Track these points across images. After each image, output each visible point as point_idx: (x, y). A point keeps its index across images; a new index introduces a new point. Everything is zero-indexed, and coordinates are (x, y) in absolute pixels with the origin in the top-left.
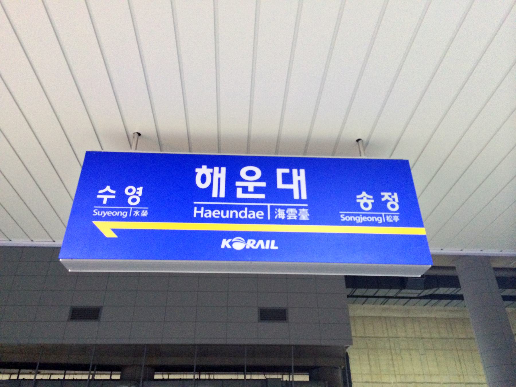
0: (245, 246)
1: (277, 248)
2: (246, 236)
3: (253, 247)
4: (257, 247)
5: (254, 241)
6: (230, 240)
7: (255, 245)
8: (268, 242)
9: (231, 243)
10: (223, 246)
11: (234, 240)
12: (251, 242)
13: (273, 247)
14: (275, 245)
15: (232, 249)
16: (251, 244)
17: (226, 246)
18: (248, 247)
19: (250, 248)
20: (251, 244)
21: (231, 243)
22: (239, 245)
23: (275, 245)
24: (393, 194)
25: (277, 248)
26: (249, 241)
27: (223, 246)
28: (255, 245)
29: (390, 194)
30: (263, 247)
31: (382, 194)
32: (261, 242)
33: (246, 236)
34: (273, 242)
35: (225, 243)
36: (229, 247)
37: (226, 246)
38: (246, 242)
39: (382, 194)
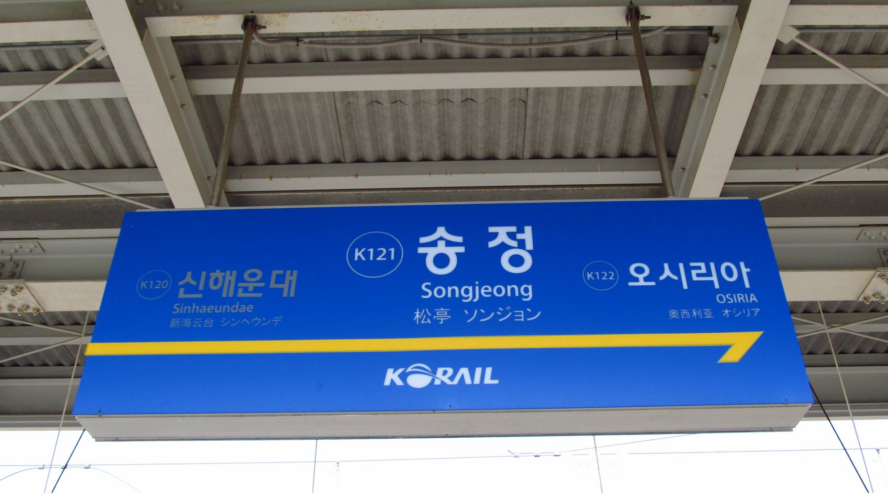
0: (433, 380)
1: (496, 382)
2: (434, 359)
3: (449, 382)
4: (456, 382)
5: (450, 371)
6: (400, 371)
7: (452, 378)
8: (478, 371)
9: (403, 377)
10: (387, 382)
11: (409, 369)
12: (445, 373)
13: (488, 380)
14: (492, 378)
16: (443, 376)
17: (392, 381)
18: (437, 382)
19: (442, 382)
21: (403, 377)
22: (418, 381)
23: (492, 378)
24: (522, 231)
25: (496, 382)
26: (440, 371)
27: (387, 382)
28: (452, 378)
29: (513, 229)
30: (468, 381)
31: (492, 229)
32: (464, 371)
33: (434, 359)
34: (489, 371)
36: (399, 382)
37: (392, 381)
38: (434, 372)
39: (492, 229)
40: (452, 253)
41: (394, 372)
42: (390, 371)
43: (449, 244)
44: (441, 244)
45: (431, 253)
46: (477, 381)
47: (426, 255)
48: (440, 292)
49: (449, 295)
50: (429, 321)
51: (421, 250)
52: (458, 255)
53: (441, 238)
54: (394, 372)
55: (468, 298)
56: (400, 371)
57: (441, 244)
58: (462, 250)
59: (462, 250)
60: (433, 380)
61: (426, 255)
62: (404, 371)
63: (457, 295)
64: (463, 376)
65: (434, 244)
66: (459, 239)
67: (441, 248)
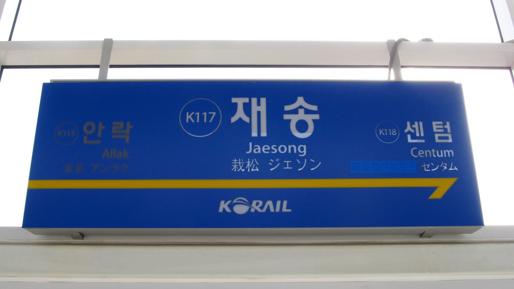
0: (250, 209)
1: (290, 210)
2: (251, 195)
3: (260, 210)
5: (261, 203)
6: (229, 202)
7: (262, 208)
8: (279, 203)
10: (221, 210)
11: (235, 201)
12: (257, 204)
13: (285, 210)
14: (287, 208)
15: (233, 212)
16: (256, 206)
17: (224, 209)
18: (253, 210)
19: (256, 210)
20: (256, 206)
21: (231, 206)
22: (241, 209)
25: (290, 210)
26: (254, 202)
27: (221, 210)
28: (262, 208)
30: (272, 210)
32: (270, 203)
34: (285, 203)
35: (224, 206)
36: (228, 210)
37: (224, 209)
38: (250, 204)
40: (309, 119)
41: (225, 203)
42: (222, 202)
43: (308, 112)
44: (301, 111)
45: (294, 119)
46: (278, 210)
47: (289, 121)
48: (283, 149)
49: (290, 152)
50: (257, 170)
51: (286, 117)
52: (314, 121)
53: (301, 107)
54: (225, 203)
55: (303, 153)
56: (229, 202)
57: (301, 111)
58: (317, 117)
59: (317, 117)
60: (250, 209)
61: (289, 121)
62: (231, 202)
63: (295, 152)
64: (268, 207)
65: (295, 112)
66: (315, 108)
67: (301, 115)
